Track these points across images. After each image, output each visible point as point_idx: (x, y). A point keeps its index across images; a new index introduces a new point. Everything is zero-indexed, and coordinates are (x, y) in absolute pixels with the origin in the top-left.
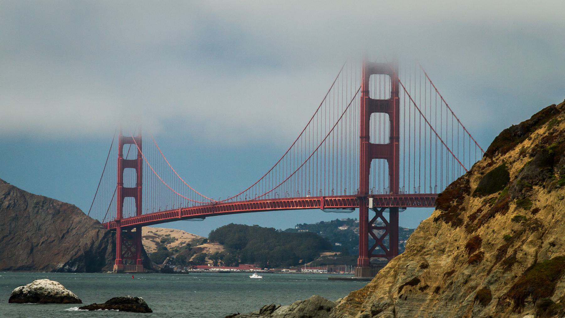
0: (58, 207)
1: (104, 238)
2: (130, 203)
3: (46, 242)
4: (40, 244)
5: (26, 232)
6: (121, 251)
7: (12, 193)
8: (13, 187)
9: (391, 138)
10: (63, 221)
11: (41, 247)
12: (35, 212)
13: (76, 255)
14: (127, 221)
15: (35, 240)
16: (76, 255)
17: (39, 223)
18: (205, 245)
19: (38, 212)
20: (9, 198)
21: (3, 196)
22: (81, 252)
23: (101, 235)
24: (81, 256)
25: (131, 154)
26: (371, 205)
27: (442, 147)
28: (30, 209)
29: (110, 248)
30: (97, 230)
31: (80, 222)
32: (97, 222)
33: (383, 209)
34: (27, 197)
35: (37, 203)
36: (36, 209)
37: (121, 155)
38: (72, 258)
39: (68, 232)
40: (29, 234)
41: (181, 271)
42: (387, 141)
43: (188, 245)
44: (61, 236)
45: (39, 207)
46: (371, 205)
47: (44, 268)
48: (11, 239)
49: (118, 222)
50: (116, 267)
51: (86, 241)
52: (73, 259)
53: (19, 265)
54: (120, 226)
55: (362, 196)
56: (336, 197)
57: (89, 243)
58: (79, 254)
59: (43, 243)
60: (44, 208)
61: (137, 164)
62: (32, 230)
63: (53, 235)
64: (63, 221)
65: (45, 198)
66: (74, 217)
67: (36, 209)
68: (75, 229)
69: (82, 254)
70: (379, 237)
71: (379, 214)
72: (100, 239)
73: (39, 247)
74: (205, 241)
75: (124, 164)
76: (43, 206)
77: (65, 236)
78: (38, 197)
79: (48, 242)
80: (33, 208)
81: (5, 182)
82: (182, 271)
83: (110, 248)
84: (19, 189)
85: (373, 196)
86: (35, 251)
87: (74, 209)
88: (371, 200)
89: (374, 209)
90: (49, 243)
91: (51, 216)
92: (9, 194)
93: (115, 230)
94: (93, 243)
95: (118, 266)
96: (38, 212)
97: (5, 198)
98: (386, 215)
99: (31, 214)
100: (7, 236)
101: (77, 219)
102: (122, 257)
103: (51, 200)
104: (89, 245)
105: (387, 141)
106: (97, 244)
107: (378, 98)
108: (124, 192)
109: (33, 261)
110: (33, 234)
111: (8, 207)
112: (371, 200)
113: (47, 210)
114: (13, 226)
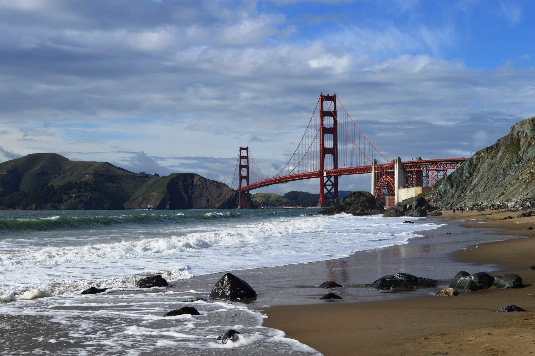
0: (218, 184)
1: (235, 195)
2: (244, 182)
6: (241, 200)
7: (201, 179)
8: (202, 177)
9: (334, 145)
10: (220, 189)
12: (210, 186)
14: (242, 189)
15: (209, 197)
17: (211, 190)
18: (282, 199)
19: (210, 186)
20: (200, 181)
23: (234, 194)
25: (244, 162)
26: (325, 175)
27: (362, 154)
28: (208, 185)
30: (232, 192)
31: (226, 190)
32: (233, 190)
33: (331, 176)
34: (207, 181)
35: (210, 183)
36: (210, 185)
37: (240, 163)
38: (222, 204)
39: (222, 194)
40: (207, 195)
42: (332, 147)
43: (277, 199)
44: (219, 195)
46: (325, 175)
48: (200, 197)
49: (240, 189)
50: (239, 207)
51: (228, 197)
53: (202, 207)
55: (321, 171)
56: (311, 172)
57: (229, 197)
58: (225, 202)
59: (212, 198)
60: (213, 184)
61: (247, 167)
63: (216, 195)
64: (220, 189)
65: (213, 181)
66: (224, 188)
70: (329, 189)
71: (329, 179)
73: (211, 199)
74: (283, 197)
75: (241, 167)
76: (212, 184)
78: (211, 180)
81: (199, 175)
83: (237, 199)
84: (204, 178)
85: (326, 171)
86: (210, 201)
87: (224, 185)
88: (325, 172)
89: (327, 176)
91: (215, 188)
92: (200, 180)
93: (239, 192)
94: (231, 197)
95: (240, 206)
96: (210, 186)
97: (199, 181)
98: (332, 179)
99: (208, 187)
100: (198, 196)
101: (225, 188)
102: (241, 202)
103: (215, 181)
104: (229, 198)
105: (332, 147)
106: (232, 198)
107: (329, 127)
108: (242, 178)
109: (208, 205)
111: (200, 184)
112: (325, 172)
114: (201, 192)
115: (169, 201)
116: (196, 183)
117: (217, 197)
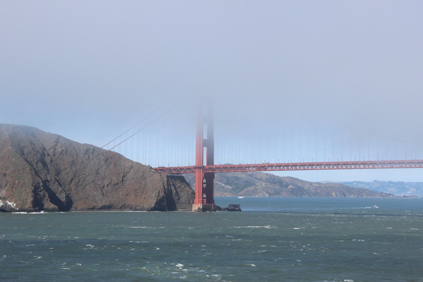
3: (110, 184)
4: (106, 186)
5: (88, 175)
11: (108, 188)
12: (87, 158)
13: (159, 196)
16: (159, 196)
19: (89, 158)
21: (55, 144)
22: (162, 194)
24: (163, 197)
29: (173, 188)
32: (151, 168)
35: (87, 150)
36: (87, 155)
39: (124, 176)
41: (234, 209)
44: (121, 179)
45: (88, 153)
47: (122, 207)
52: (159, 199)
54: (203, 171)
62: (93, 174)
67: (87, 155)
68: (129, 173)
69: (164, 195)
72: (166, 182)
76: (93, 153)
77: (124, 179)
79: (112, 184)
80: (84, 155)
82: (237, 209)
83: (173, 188)
90: (113, 185)
96: (89, 158)
106: (166, 187)
110: (95, 177)
113: (98, 156)
115: (46, 192)
116: (53, 150)
117: (118, 184)
